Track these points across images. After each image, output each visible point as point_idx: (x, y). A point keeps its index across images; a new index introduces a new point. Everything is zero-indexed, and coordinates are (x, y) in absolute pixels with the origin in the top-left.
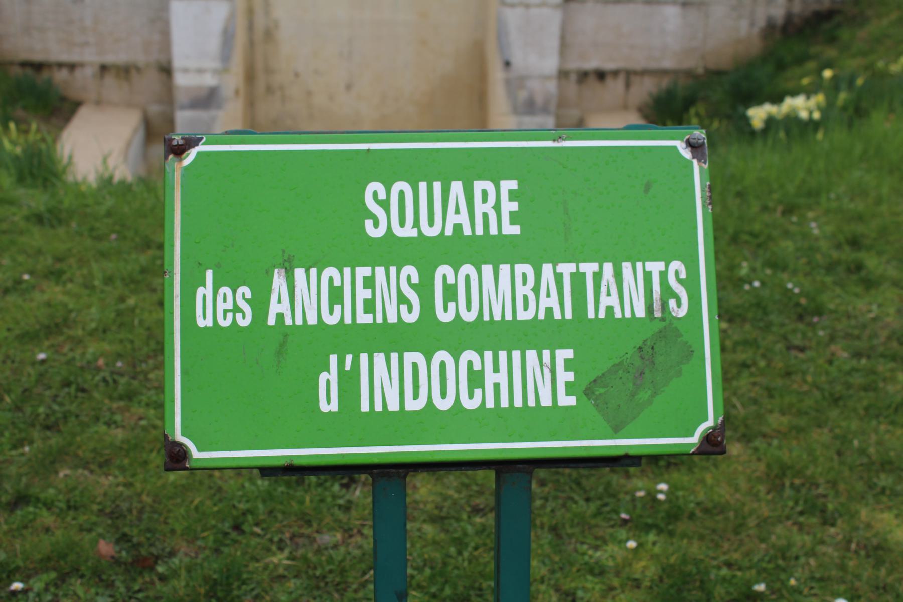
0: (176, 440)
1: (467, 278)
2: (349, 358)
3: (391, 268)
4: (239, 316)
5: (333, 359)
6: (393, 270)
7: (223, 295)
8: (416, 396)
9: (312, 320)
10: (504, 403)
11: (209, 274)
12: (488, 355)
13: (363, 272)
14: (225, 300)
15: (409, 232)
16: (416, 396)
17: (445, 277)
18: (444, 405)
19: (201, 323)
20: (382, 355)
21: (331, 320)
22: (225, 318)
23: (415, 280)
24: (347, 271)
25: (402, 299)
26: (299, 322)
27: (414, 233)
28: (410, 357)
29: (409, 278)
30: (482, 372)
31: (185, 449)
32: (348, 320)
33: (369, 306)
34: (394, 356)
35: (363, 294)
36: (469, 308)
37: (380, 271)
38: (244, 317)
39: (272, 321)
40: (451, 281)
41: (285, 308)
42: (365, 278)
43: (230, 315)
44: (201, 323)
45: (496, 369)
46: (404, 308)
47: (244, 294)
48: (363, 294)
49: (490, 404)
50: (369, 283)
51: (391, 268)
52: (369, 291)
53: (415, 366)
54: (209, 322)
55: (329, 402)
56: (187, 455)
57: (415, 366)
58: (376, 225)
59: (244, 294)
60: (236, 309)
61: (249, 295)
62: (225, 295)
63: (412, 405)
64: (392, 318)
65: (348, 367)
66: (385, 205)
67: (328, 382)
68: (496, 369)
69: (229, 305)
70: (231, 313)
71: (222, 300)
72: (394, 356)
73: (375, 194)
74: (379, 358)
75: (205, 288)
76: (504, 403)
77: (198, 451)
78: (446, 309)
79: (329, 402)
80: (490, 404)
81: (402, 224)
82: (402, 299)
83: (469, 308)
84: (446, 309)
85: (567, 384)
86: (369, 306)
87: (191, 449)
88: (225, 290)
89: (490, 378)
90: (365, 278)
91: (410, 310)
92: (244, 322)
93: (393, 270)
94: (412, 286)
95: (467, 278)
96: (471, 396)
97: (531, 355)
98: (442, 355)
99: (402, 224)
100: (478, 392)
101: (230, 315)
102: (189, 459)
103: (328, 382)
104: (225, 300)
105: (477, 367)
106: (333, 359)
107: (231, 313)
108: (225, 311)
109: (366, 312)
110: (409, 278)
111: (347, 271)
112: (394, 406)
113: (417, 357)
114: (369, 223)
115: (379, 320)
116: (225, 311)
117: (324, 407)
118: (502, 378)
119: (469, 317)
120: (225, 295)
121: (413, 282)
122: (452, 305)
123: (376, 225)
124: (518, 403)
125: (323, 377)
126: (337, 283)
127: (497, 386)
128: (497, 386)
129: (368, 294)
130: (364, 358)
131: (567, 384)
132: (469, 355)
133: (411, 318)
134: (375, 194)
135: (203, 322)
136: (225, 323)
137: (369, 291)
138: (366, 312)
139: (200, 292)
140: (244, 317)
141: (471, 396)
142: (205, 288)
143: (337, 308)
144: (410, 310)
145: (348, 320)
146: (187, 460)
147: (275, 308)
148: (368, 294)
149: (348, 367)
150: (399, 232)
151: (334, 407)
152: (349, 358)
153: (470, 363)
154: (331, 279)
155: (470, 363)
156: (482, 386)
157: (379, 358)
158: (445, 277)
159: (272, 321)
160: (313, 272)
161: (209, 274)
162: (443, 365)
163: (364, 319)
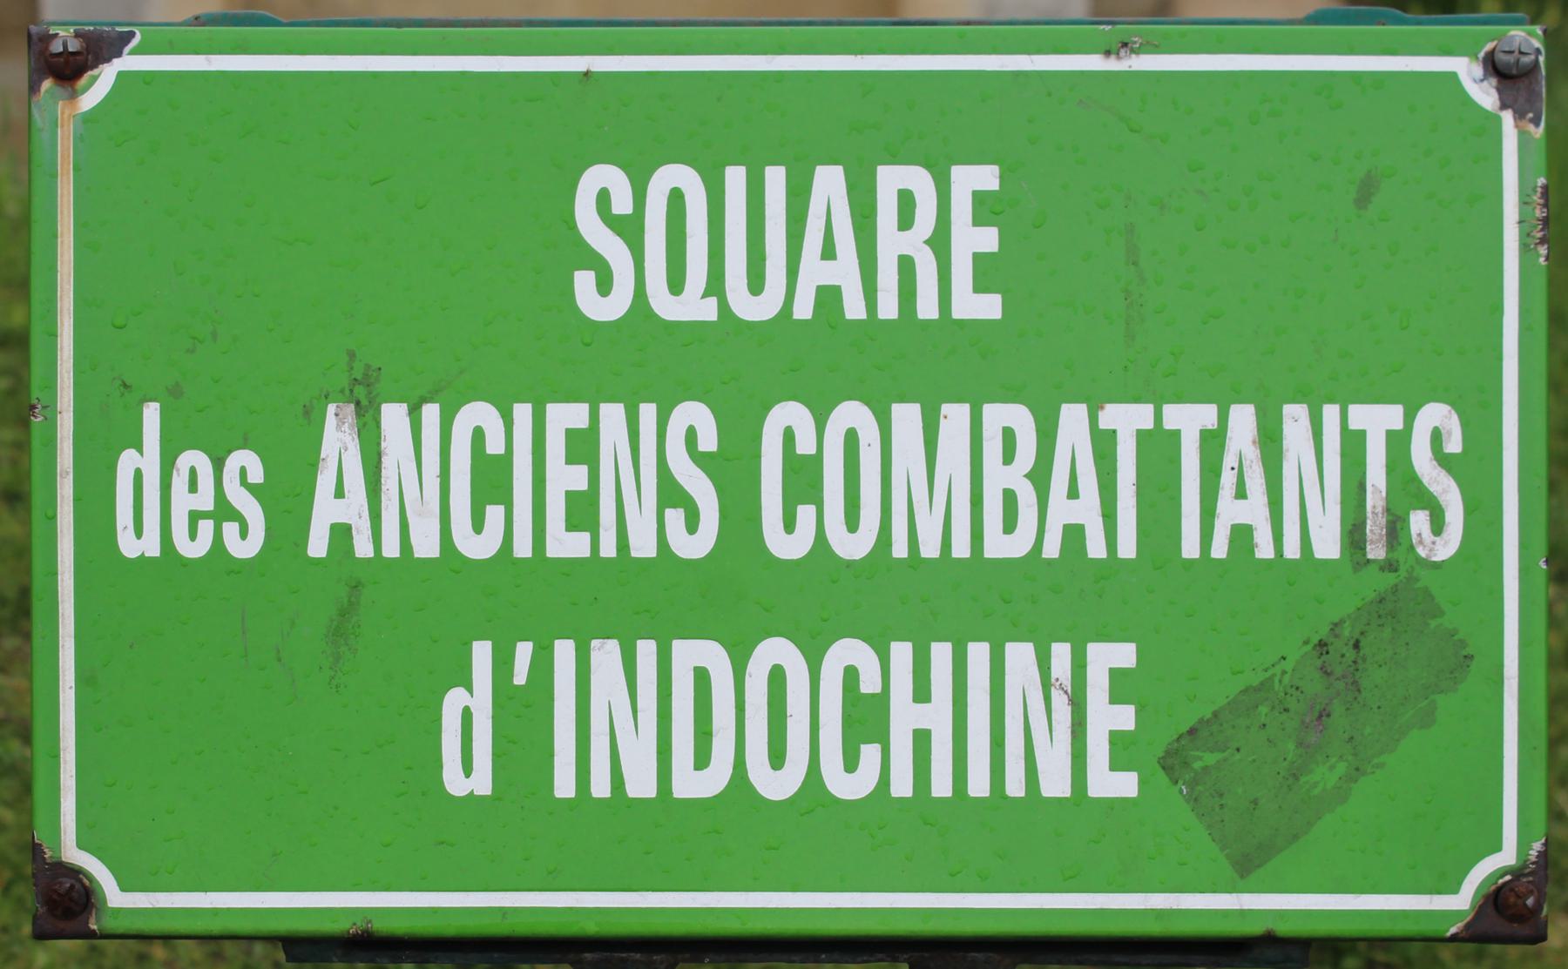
1: (851, 438)
8: (702, 759)
12: (901, 653)
13: (566, 416)
15: (693, 307)
16: (702, 759)
17: (789, 436)
18: (777, 785)
23: (708, 442)
24: (523, 413)
25: (671, 493)
27: (707, 311)
28: (691, 653)
29: (691, 436)
30: (882, 701)
32: (523, 548)
33: (582, 511)
35: (565, 478)
36: (852, 523)
37: (613, 415)
42: (571, 434)
45: (922, 693)
46: (675, 518)
48: (565, 478)
49: (902, 786)
50: (583, 447)
53: (702, 677)
57: (702, 677)
58: (604, 285)
63: (692, 784)
68: (922, 693)
72: (646, 650)
74: (606, 654)
78: (789, 525)
80: (902, 786)
81: (676, 284)
82: (671, 493)
83: (852, 523)
84: (789, 525)
86: (582, 511)
89: (904, 716)
90: (571, 434)
91: (692, 526)
95: (851, 438)
96: (851, 764)
97: (1020, 655)
99: (676, 284)
100: (870, 754)
105: (870, 683)
109: (571, 526)
110: (691, 436)
111: (523, 413)
113: (710, 654)
115: (608, 549)
118: (937, 716)
119: (853, 546)
121: (701, 449)
122: (806, 513)
123: (604, 285)
127: (922, 739)
128: (922, 739)
129: (578, 478)
130: (564, 651)
133: (694, 546)
138: (571, 526)
141: (851, 764)
144: (692, 526)
145: (523, 548)
148: (578, 478)
150: (666, 307)
153: (851, 675)
155: (851, 675)
156: (882, 737)
157: (606, 654)
158: (789, 436)
162: (777, 677)
163: (567, 545)
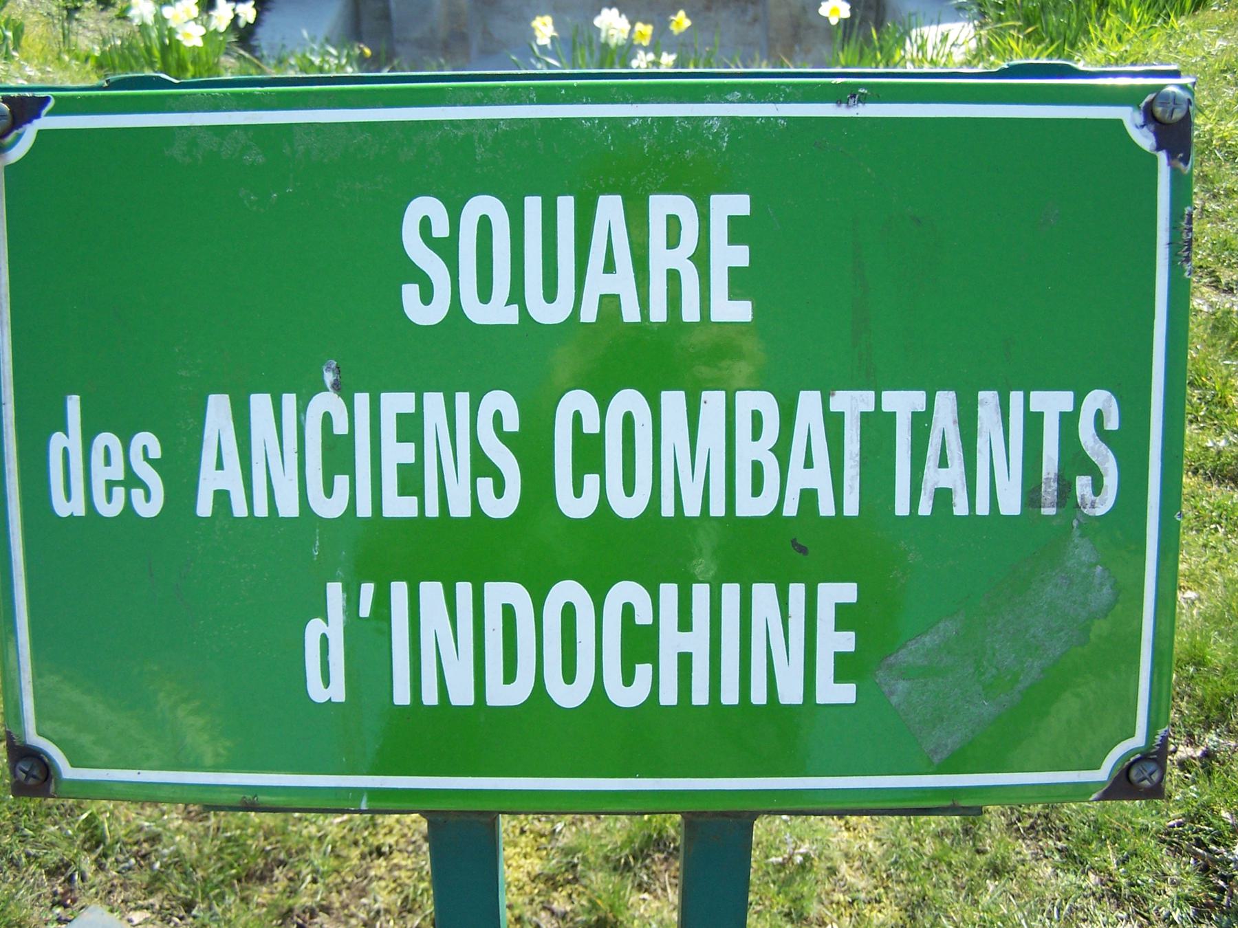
0: (28, 743)
1: (628, 420)
2: (368, 591)
3: (458, 394)
4: (137, 494)
5: (335, 592)
6: (289, 401)
7: (141, 449)
8: (510, 675)
9: (289, 508)
10: (700, 696)
11: (74, 405)
12: (669, 592)
13: (397, 403)
14: (108, 462)
15: (500, 313)
16: (510, 675)
17: (577, 418)
18: (568, 696)
19: (63, 508)
20: (437, 587)
21: (330, 508)
22: (109, 499)
23: (512, 423)
24: (362, 400)
25: (482, 466)
26: (261, 510)
27: (511, 316)
28: (500, 593)
29: (498, 418)
30: (652, 631)
31: (46, 760)
32: (364, 509)
33: (411, 480)
34: (464, 590)
35: (397, 453)
36: (629, 489)
37: (434, 402)
38: (148, 497)
39: (205, 508)
40: (591, 426)
41: (231, 480)
42: (401, 417)
43: (119, 492)
44: (63, 508)
45: (685, 624)
46: (485, 484)
47: (145, 448)
48: (397, 453)
49: (669, 696)
50: (411, 428)
51: (458, 394)
52: (410, 447)
53: (509, 613)
54: (77, 508)
55: (326, 682)
56: (52, 773)
57: (509, 613)
58: (427, 297)
59: (145, 448)
60: (132, 480)
61: (156, 452)
62: (107, 449)
63: (502, 695)
64: (460, 508)
65: (365, 610)
66: (447, 249)
67: (324, 640)
68: (685, 624)
69: (117, 472)
70: (122, 490)
71: (102, 462)
72: (464, 590)
73: (425, 224)
74: (431, 592)
75: (67, 434)
76: (700, 696)
77: (72, 766)
78: (578, 491)
79: (326, 682)
80: (669, 696)
81: (485, 294)
82: (482, 466)
83: (629, 489)
84: (578, 491)
85: (840, 657)
86: (411, 480)
87: (58, 761)
88: (107, 439)
89: (671, 642)
90: (401, 417)
91: (499, 491)
92: (149, 508)
93: (289, 401)
94: (505, 438)
95: (628, 420)
96: (628, 679)
97: (764, 593)
98: (568, 591)
99: (485, 294)
100: (643, 671)
101: (119, 492)
102: (56, 780)
103: (324, 640)
104: (108, 462)
105: (643, 617)
106: (335, 592)
107: (122, 490)
108: (110, 484)
109: (403, 492)
110: (498, 418)
111: (362, 400)
112: (462, 695)
113: (515, 594)
114: (410, 292)
115: (432, 511)
116: (110, 484)
117: (317, 692)
118: (697, 642)
119: (629, 508)
120: (107, 449)
121: (505, 429)
122: (592, 481)
123: (427, 297)
124: (730, 696)
125: (314, 629)
126: (341, 428)
127: (685, 661)
128: (685, 661)
129: (407, 452)
130: (399, 590)
131: (840, 657)
132: (626, 592)
133: (501, 508)
134: (425, 224)
135: (67, 506)
136: (110, 509)
137: (410, 447)
138: (403, 492)
139: (57, 441)
140: (148, 497)
141: (628, 679)
142: (67, 434)
143: (341, 481)
144: (499, 491)
145: (364, 509)
146: (53, 780)
147: (210, 482)
148: (407, 452)
149: (365, 610)
150: (477, 313)
151: (337, 691)
152: (368, 591)
153: (628, 610)
154: (327, 419)
155: (628, 610)
156: (652, 657)
157: (431, 592)
158: (577, 418)
159: (205, 508)
160: (289, 401)
161: (74, 405)
162: (569, 612)
163: (399, 507)
